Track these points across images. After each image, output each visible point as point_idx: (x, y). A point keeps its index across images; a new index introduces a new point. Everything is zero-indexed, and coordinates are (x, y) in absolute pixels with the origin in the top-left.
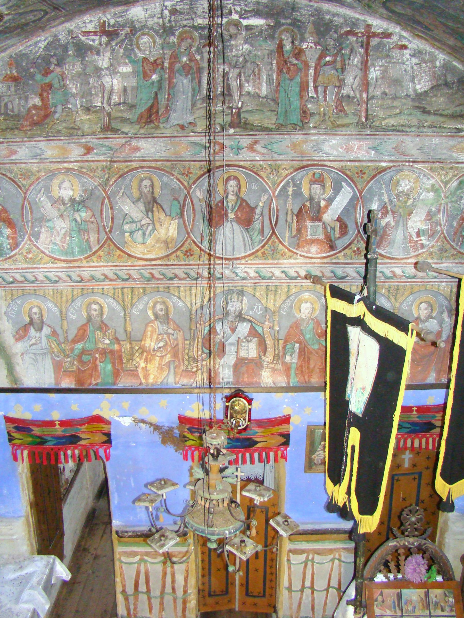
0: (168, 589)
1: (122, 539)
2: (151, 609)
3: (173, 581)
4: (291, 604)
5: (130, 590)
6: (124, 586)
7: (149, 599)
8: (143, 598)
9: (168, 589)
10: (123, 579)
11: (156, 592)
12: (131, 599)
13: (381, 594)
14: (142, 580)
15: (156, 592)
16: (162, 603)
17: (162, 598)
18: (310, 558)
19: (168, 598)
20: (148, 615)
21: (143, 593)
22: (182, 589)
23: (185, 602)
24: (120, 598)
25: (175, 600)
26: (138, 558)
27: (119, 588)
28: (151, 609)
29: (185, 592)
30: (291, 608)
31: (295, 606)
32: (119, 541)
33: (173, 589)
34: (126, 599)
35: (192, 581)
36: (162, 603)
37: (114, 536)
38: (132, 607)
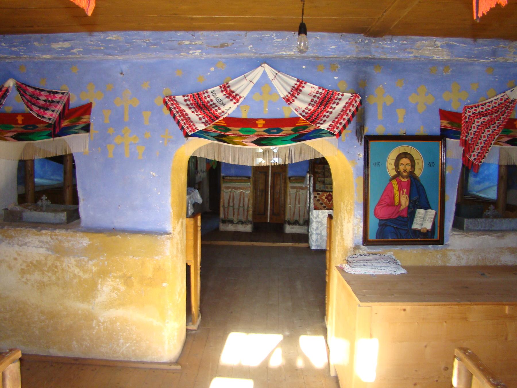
0: (241, 205)
1: (225, 180)
2: (234, 214)
3: (244, 201)
4: (291, 213)
5: (226, 205)
6: (224, 203)
7: (234, 209)
8: (231, 208)
9: (241, 205)
10: (224, 200)
11: (236, 206)
12: (226, 209)
13: (318, 166)
14: (231, 200)
15: (236, 206)
16: (238, 212)
17: (239, 209)
18: (298, 191)
19: (241, 209)
20: (233, 218)
21: (231, 206)
22: (247, 205)
23: (248, 211)
24: (222, 209)
25: (244, 210)
26: (230, 190)
27: (222, 204)
28: (234, 214)
29: (248, 206)
30: (291, 215)
31: (292, 213)
32: (223, 181)
33: (243, 204)
34: (224, 210)
35: (251, 201)
36: (238, 212)
37: (222, 179)
38: (226, 214)
